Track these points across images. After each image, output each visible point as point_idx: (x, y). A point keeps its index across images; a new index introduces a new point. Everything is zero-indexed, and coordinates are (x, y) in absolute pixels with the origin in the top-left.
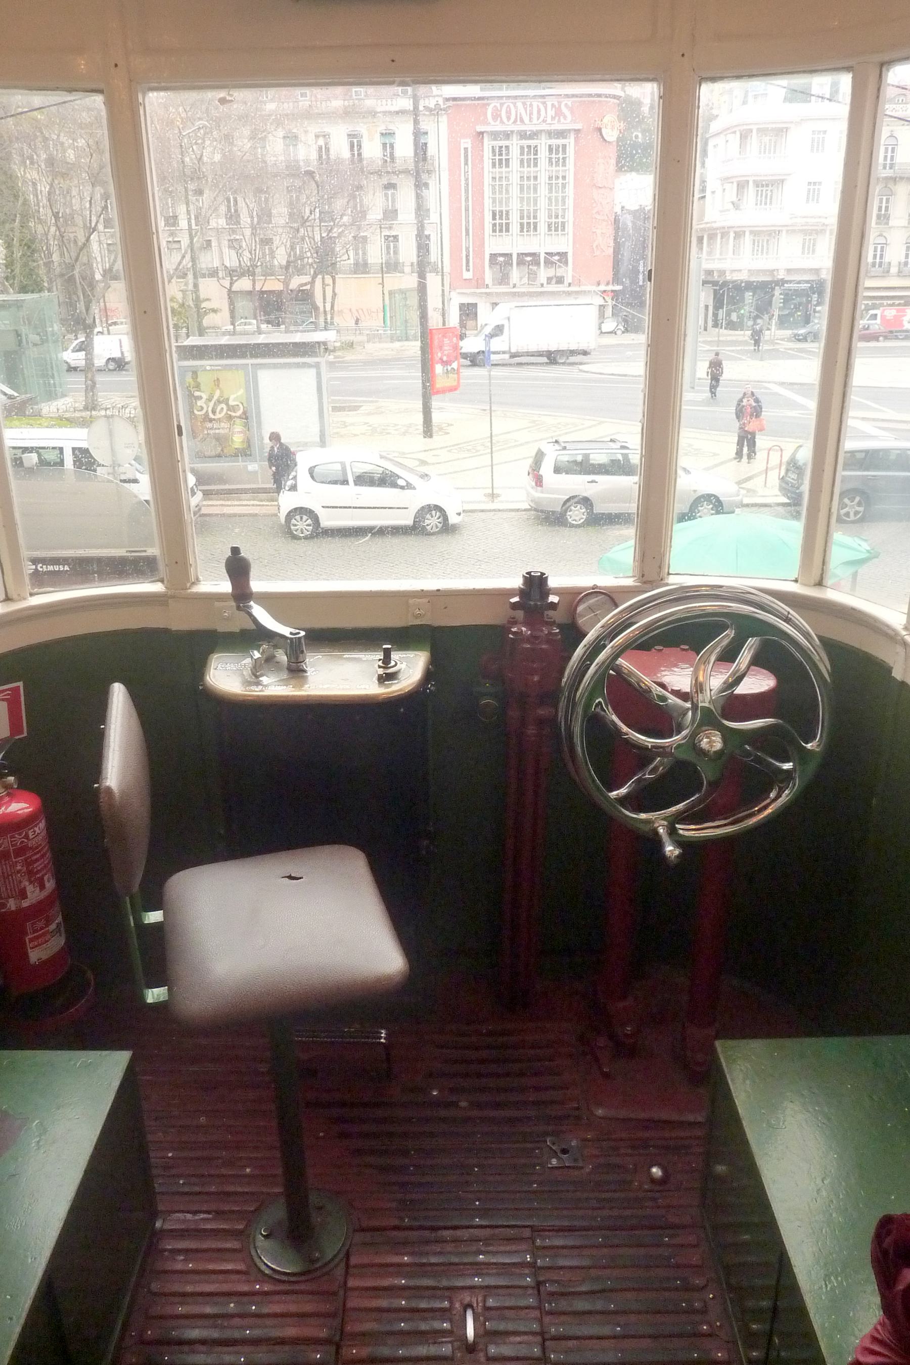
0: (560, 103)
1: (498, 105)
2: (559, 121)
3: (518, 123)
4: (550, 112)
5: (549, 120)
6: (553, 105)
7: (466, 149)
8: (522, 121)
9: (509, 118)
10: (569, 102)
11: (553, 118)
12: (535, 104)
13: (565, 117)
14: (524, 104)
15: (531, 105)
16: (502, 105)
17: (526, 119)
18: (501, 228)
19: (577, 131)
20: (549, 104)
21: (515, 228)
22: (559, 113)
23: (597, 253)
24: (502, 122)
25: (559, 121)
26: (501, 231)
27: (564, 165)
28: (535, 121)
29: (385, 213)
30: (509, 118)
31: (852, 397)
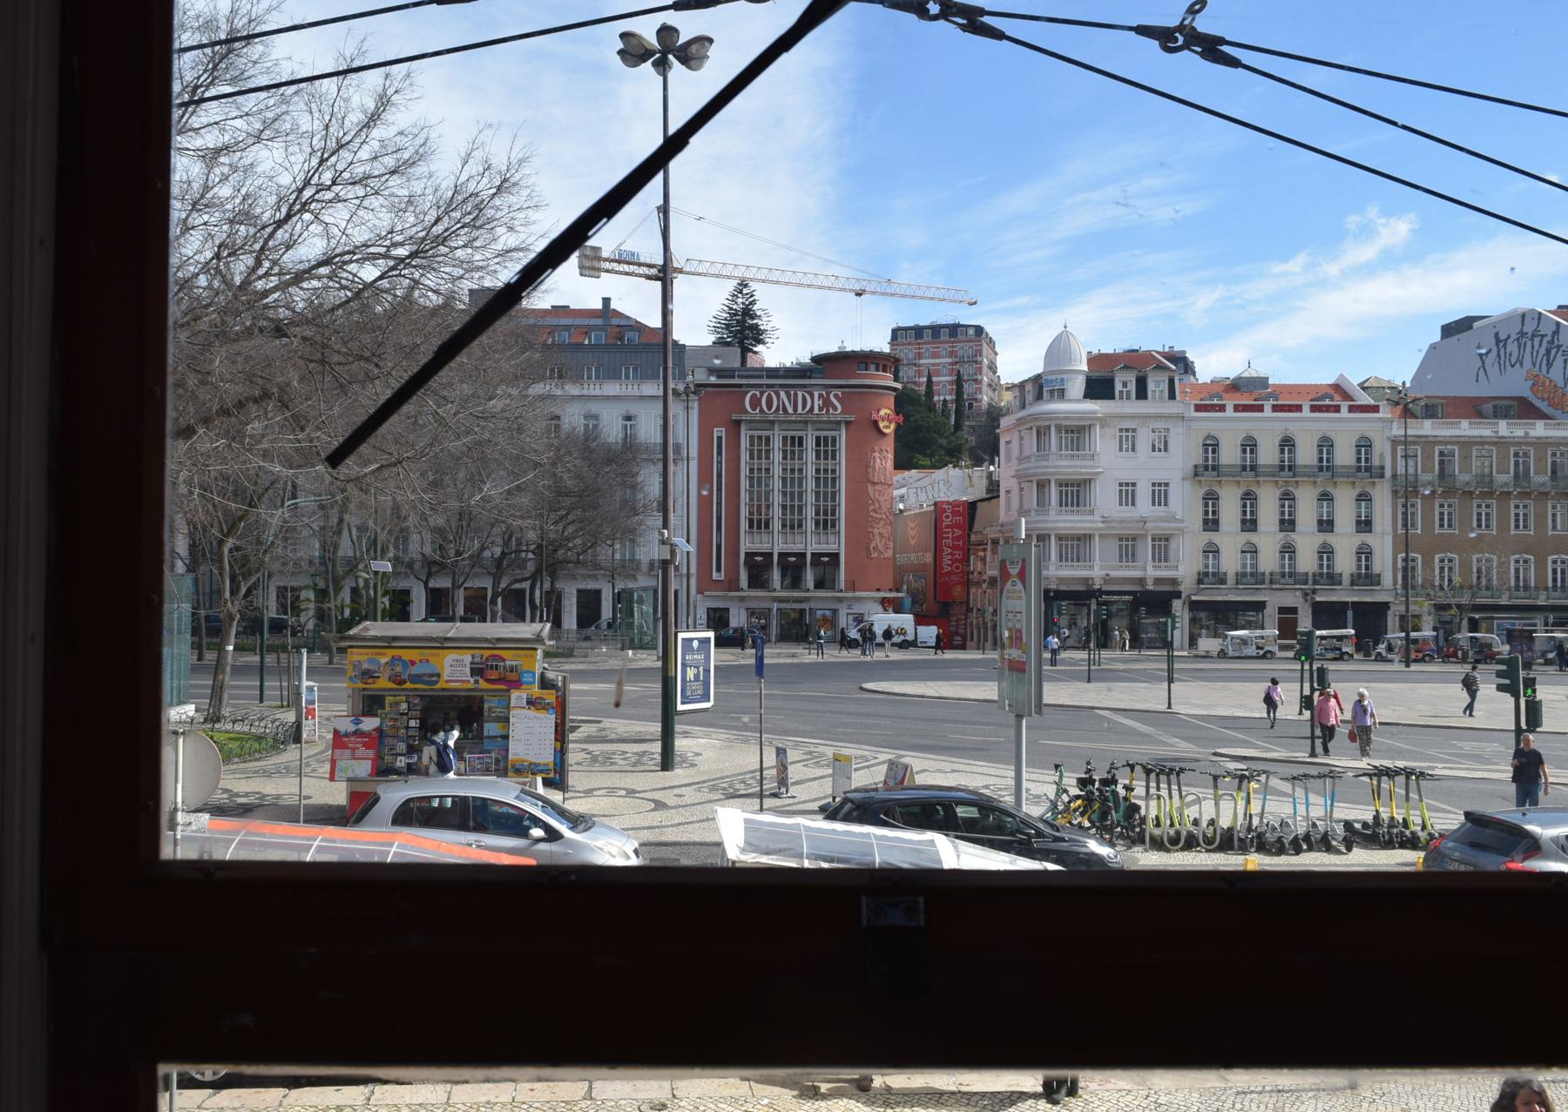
0: (828, 394)
6: (820, 396)
7: (720, 438)
9: (769, 408)
11: (820, 409)
12: (800, 394)
13: (835, 409)
16: (762, 393)
17: (790, 410)
18: (760, 524)
19: (848, 423)
20: (816, 394)
22: (827, 403)
23: (875, 555)
24: (762, 411)
26: (759, 527)
27: (834, 458)
30: (769, 408)
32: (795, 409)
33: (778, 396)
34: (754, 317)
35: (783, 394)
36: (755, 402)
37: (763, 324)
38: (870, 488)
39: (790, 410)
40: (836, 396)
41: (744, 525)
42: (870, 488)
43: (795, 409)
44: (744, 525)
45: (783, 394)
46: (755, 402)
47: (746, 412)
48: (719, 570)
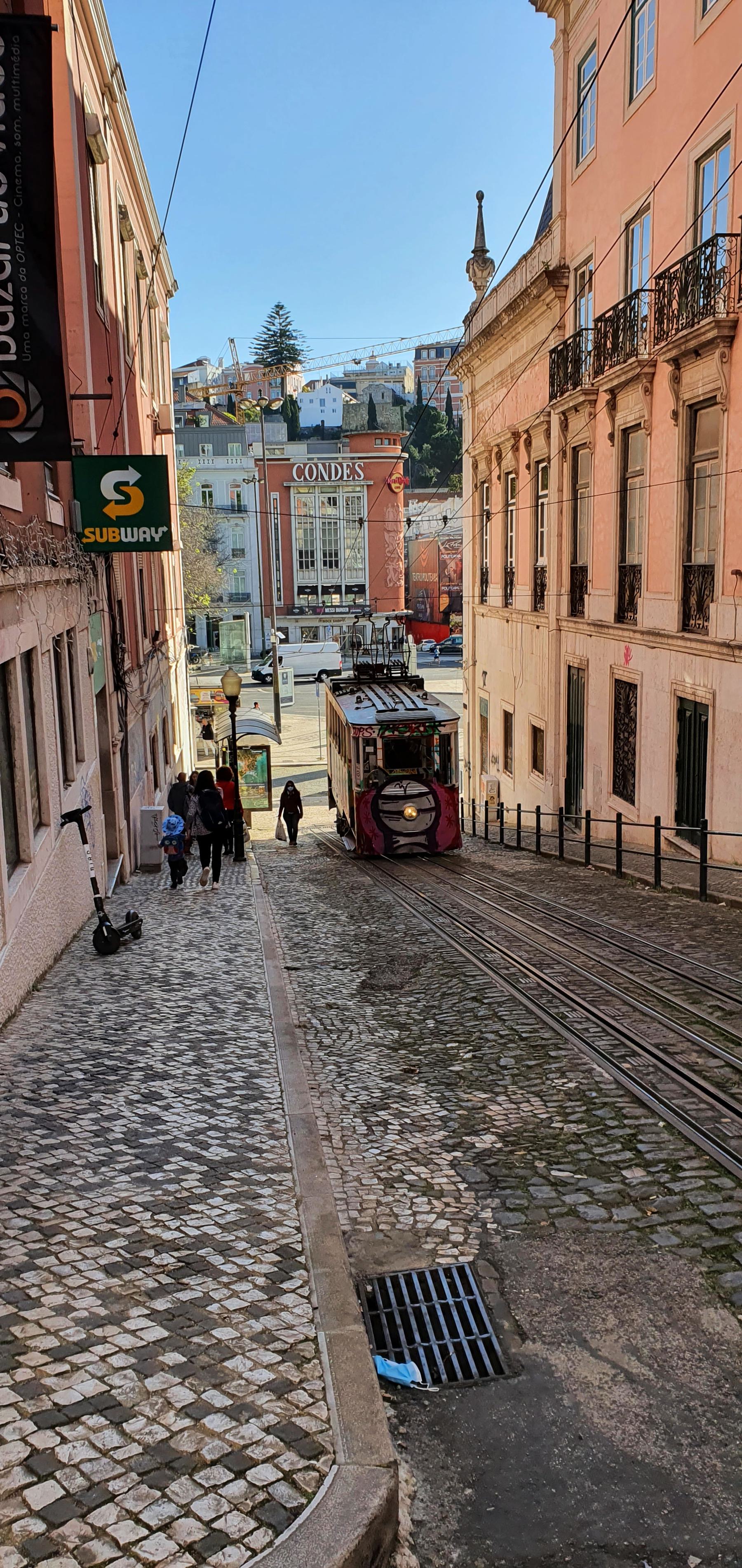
0: (354, 464)
2: (354, 479)
4: (346, 471)
5: (345, 478)
6: (348, 466)
8: (323, 478)
9: (311, 476)
10: (361, 462)
11: (348, 476)
13: (359, 476)
14: (324, 465)
15: (330, 466)
16: (305, 465)
17: (326, 478)
19: (368, 486)
21: (319, 564)
24: (305, 479)
25: (354, 479)
28: (333, 478)
30: (311, 476)
31: (362, 1328)
32: (330, 477)
33: (317, 467)
34: (290, 337)
35: (320, 466)
36: (301, 472)
37: (298, 344)
38: (386, 535)
39: (326, 478)
40: (359, 466)
41: (296, 565)
42: (386, 535)
43: (330, 477)
44: (296, 565)
45: (320, 466)
46: (301, 472)
47: (294, 480)
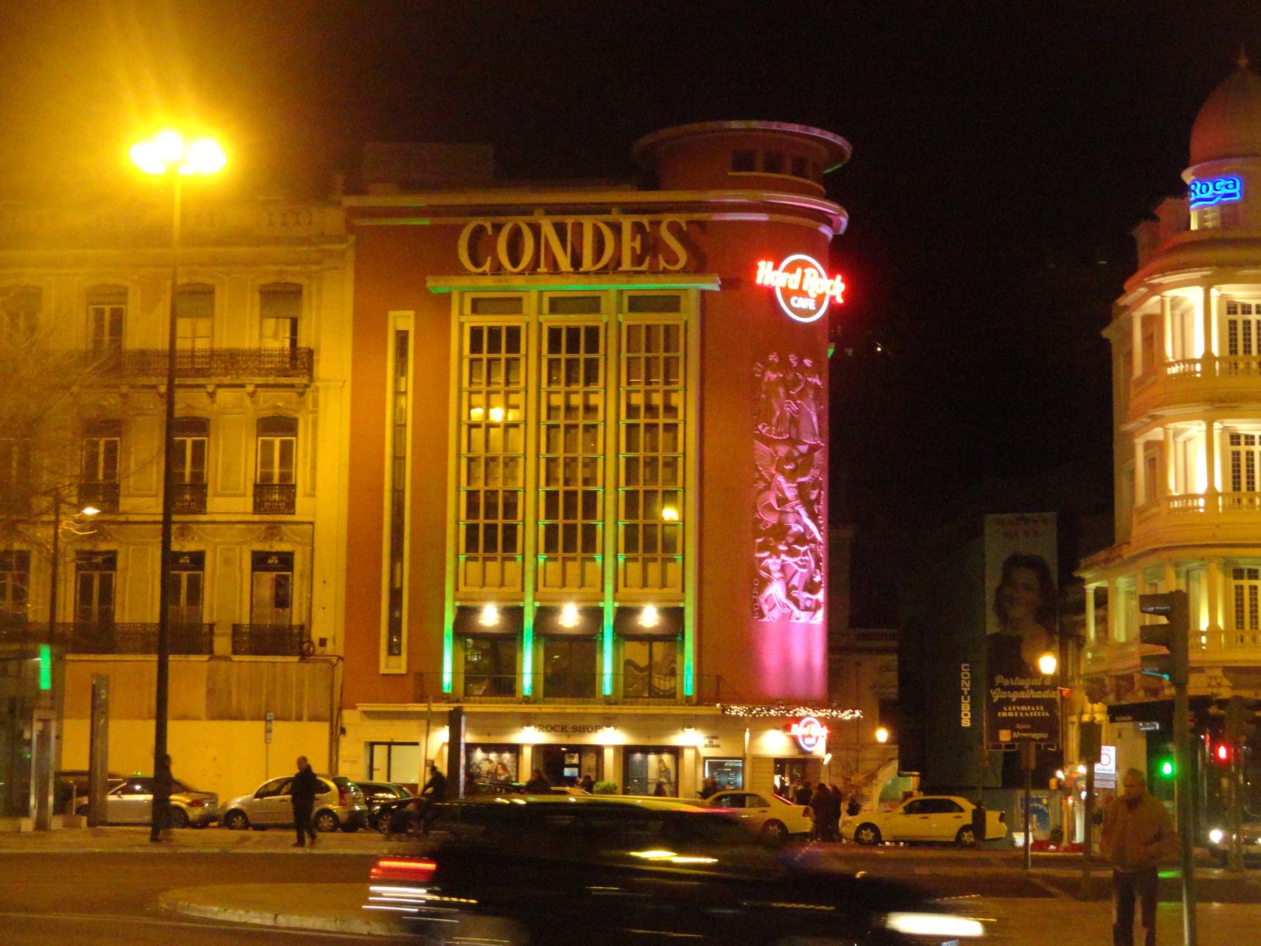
1: (488, 225)
3: (542, 269)
4: (630, 244)
5: (626, 264)
6: (638, 228)
9: (515, 261)
10: (682, 219)
11: (638, 260)
13: (672, 259)
14: (560, 230)
15: (579, 227)
16: (498, 228)
20: (627, 223)
24: (498, 269)
28: (587, 263)
29: (262, 488)
32: (576, 262)
33: (536, 230)
39: (565, 263)
40: (675, 229)
43: (576, 262)
48: (393, 650)
